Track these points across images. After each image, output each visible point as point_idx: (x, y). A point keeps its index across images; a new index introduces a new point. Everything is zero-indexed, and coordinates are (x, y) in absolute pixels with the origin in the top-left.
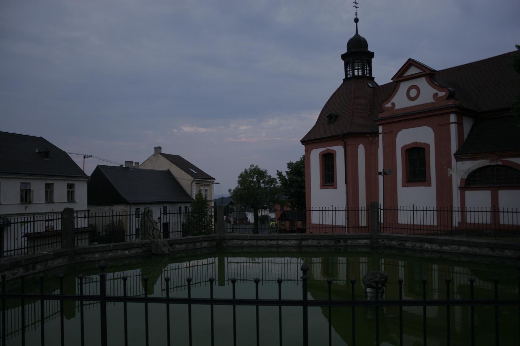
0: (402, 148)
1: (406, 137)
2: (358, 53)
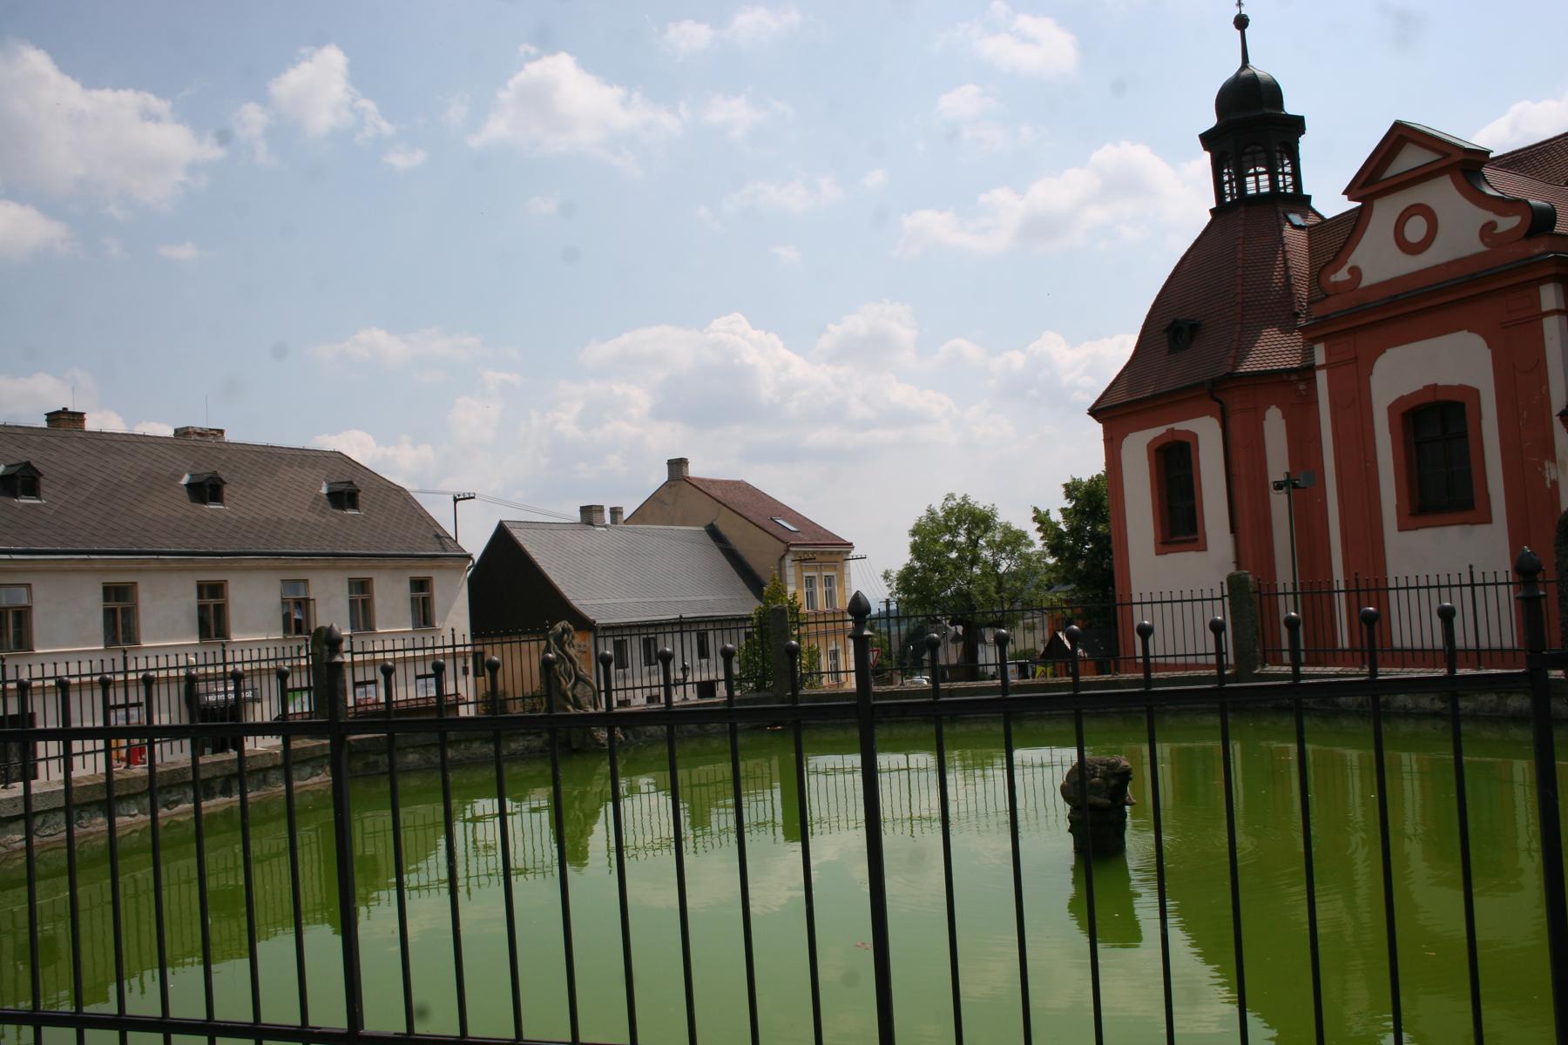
0: (1391, 408)
2: (1252, 125)
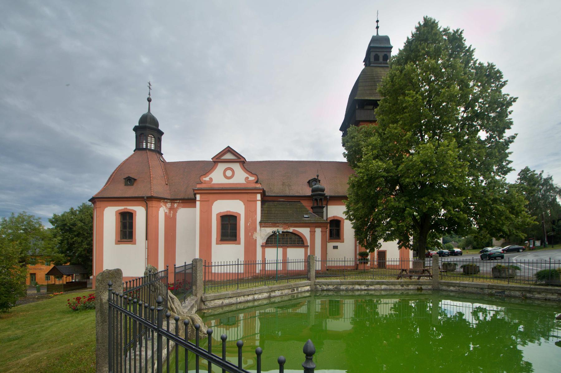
0: (217, 215)
1: (222, 206)
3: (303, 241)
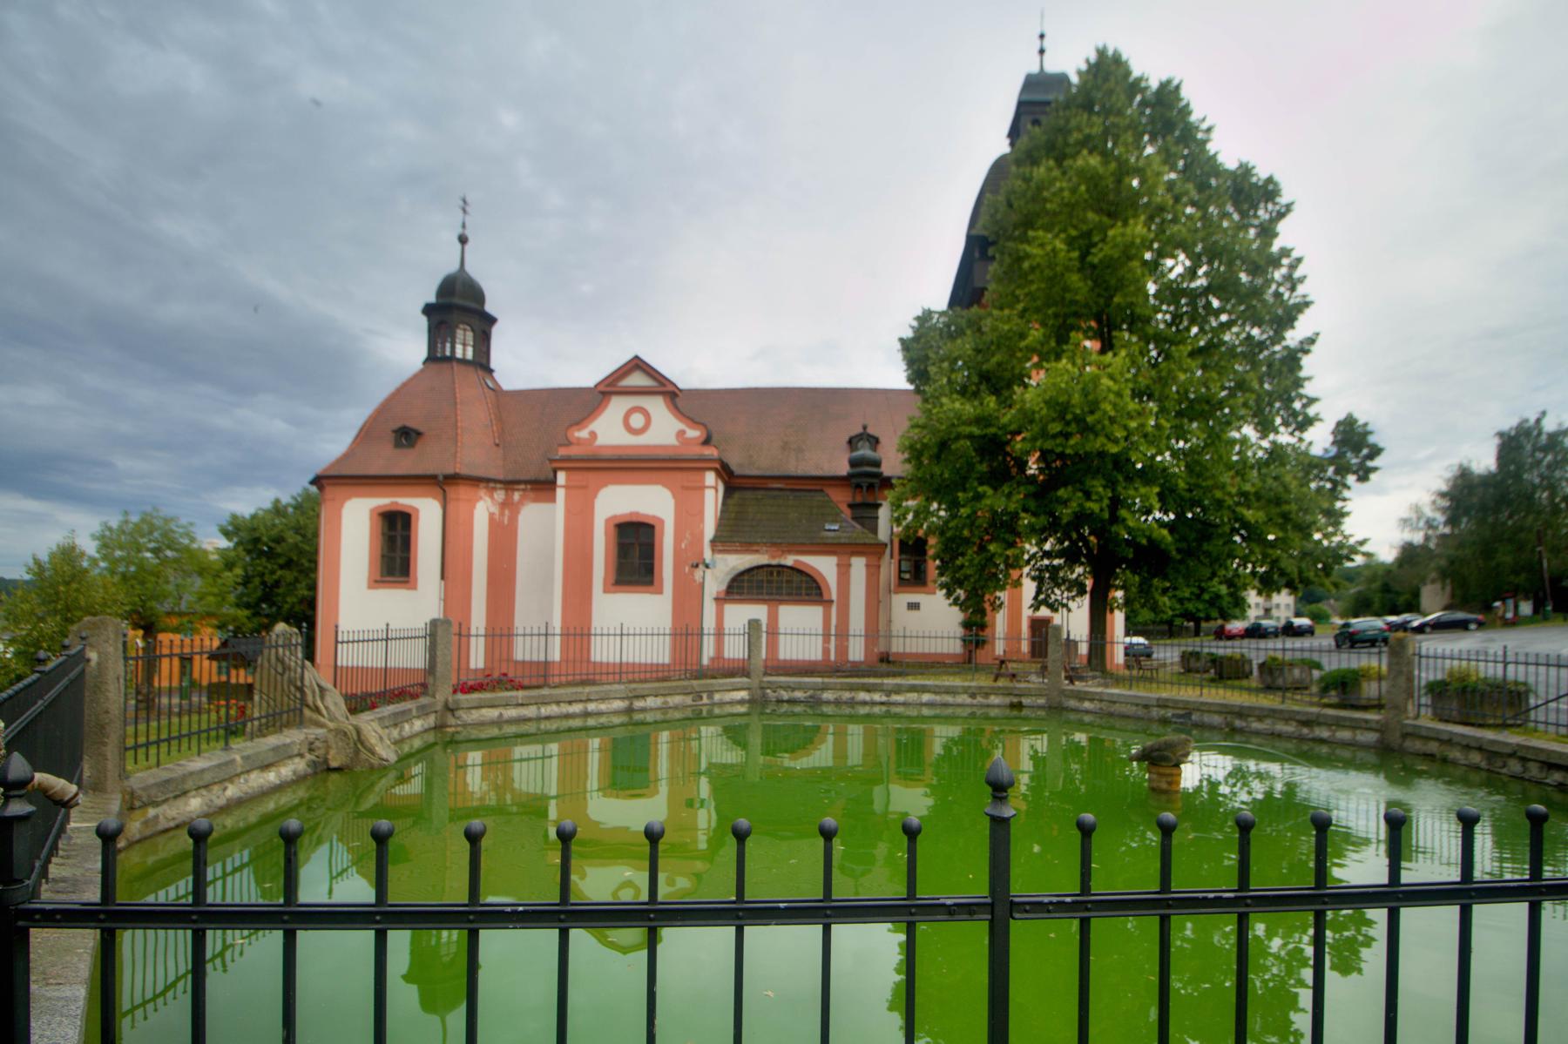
0: (608, 521)
3: (819, 588)
